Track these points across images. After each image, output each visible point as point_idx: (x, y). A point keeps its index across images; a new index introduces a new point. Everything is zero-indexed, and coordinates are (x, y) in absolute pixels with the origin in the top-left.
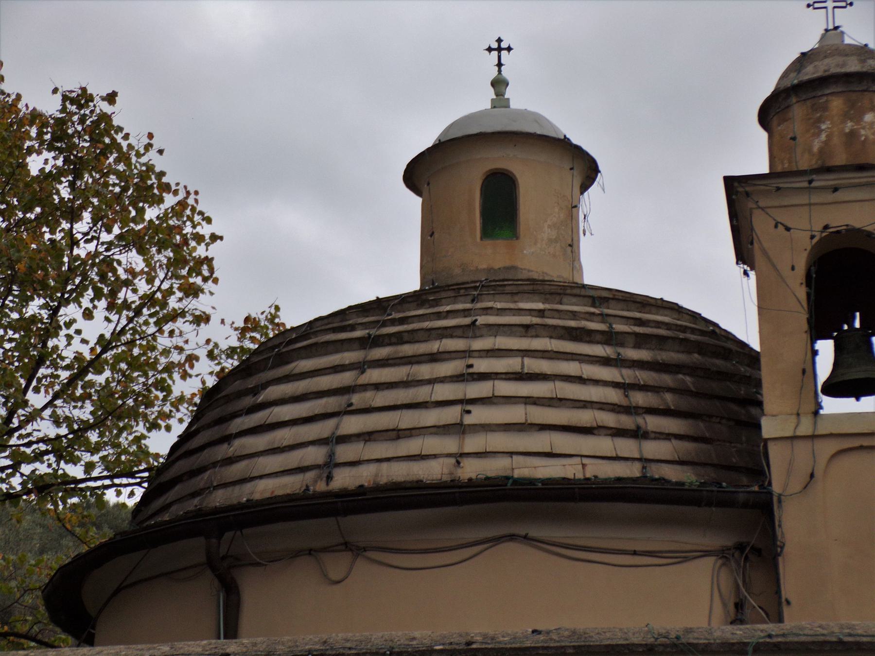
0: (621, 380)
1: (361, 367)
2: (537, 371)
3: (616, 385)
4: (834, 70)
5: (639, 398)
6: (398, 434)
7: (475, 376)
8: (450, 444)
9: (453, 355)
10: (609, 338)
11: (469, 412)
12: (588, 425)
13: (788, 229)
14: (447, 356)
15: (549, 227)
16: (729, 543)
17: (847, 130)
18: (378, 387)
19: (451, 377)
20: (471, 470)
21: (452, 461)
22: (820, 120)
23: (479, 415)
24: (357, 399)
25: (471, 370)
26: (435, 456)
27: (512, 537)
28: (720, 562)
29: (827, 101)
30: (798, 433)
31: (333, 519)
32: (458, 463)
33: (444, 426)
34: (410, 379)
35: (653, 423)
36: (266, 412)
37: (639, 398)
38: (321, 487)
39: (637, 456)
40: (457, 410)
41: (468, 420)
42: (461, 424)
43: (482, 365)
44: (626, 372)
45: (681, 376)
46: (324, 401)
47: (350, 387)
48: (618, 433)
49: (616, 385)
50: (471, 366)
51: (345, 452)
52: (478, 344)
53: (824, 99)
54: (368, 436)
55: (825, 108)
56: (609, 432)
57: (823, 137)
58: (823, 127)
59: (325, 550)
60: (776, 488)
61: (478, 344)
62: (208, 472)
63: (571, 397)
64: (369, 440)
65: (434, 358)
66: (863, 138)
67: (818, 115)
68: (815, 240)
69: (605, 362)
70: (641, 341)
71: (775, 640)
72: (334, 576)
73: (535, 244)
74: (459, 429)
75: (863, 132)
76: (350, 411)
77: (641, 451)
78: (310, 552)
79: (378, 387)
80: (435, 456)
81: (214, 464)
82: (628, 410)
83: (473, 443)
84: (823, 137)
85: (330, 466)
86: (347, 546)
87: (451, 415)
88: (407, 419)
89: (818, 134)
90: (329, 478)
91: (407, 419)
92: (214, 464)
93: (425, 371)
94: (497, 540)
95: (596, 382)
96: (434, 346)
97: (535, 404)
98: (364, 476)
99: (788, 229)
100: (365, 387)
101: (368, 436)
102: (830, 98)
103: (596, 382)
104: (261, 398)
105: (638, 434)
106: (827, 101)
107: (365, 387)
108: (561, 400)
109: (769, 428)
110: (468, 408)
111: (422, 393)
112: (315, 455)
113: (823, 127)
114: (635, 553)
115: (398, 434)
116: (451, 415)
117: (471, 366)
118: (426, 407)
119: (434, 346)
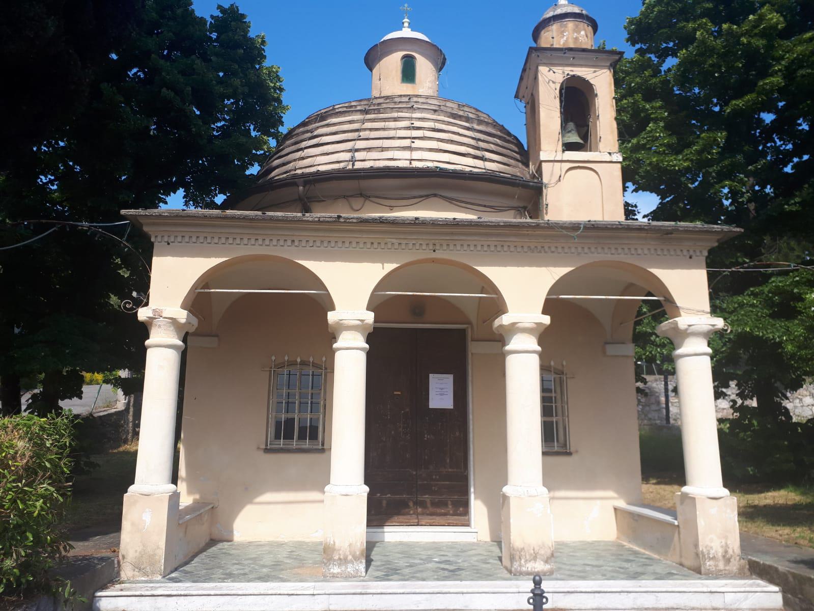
0: (474, 137)
1: (363, 121)
2: (441, 128)
3: (473, 138)
4: (569, 11)
5: (481, 144)
6: (383, 149)
7: (415, 128)
8: (406, 154)
9: (404, 119)
10: (467, 119)
11: (413, 142)
12: (464, 153)
13: (554, 73)
14: (401, 119)
15: (429, 82)
16: (522, 205)
17: (575, 37)
18: (371, 130)
19: (405, 128)
20: (416, 164)
21: (408, 162)
22: (563, 32)
23: (418, 144)
24: (363, 134)
25: (413, 125)
26: (400, 159)
27: (435, 195)
28: (517, 212)
29: (567, 24)
30: (556, 159)
31: (357, 181)
32: (411, 163)
33: (403, 147)
34: (386, 127)
35: (488, 155)
36: (319, 139)
37: (481, 144)
38: (350, 167)
39: (484, 168)
40: (409, 140)
41: (413, 145)
42: (410, 147)
43: (417, 124)
44: (476, 134)
45: (495, 139)
46: (346, 134)
47: (358, 129)
48: (475, 157)
49: (473, 138)
50: (413, 124)
51: (358, 156)
52: (415, 115)
53: (565, 23)
54: (369, 149)
55: (566, 26)
56: (472, 156)
57: (565, 38)
58: (565, 34)
59: (351, 196)
60: (545, 180)
61: (415, 115)
62: (292, 163)
63: (456, 140)
64: (369, 152)
65: (395, 119)
66: (580, 41)
67: (563, 29)
68: (565, 78)
69: (468, 129)
70: (480, 122)
71: (592, 223)
72: (355, 208)
73: (423, 88)
74: (409, 148)
75: (580, 38)
76: (359, 139)
77: (484, 165)
78: (345, 197)
79: (371, 130)
80: (400, 159)
81: (295, 160)
82: (477, 148)
83: (416, 155)
84: (565, 38)
85: (353, 160)
86: (361, 195)
87: (407, 143)
88: (387, 143)
89: (563, 37)
90: (353, 165)
91: (387, 143)
92: (295, 160)
93: (392, 124)
94: (427, 196)
95: (465, 136)
96: (395, 115)
97: (441, 142)
98: (367, 165)
99: (554, 73)
100: (365, 129)
101: (369, 149)
102: (568, 22)
103: (465, 136)
104: (316, 133)
105: (482, 158)
106: (567, 24)
107: (365, 129)
108: (452, 141)
109: (543, 156)
110: (413, 140)
111: (391, 133)
112: (347, 156)
113: (565, 34)
114: (485, 206)
115: (383, 149)
116: (407, 143)
117: (413, 124)
118: (394, 139)
119: (395, 115)
